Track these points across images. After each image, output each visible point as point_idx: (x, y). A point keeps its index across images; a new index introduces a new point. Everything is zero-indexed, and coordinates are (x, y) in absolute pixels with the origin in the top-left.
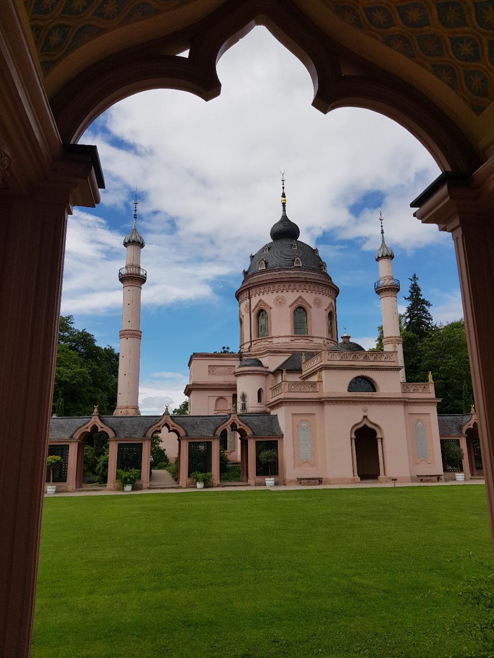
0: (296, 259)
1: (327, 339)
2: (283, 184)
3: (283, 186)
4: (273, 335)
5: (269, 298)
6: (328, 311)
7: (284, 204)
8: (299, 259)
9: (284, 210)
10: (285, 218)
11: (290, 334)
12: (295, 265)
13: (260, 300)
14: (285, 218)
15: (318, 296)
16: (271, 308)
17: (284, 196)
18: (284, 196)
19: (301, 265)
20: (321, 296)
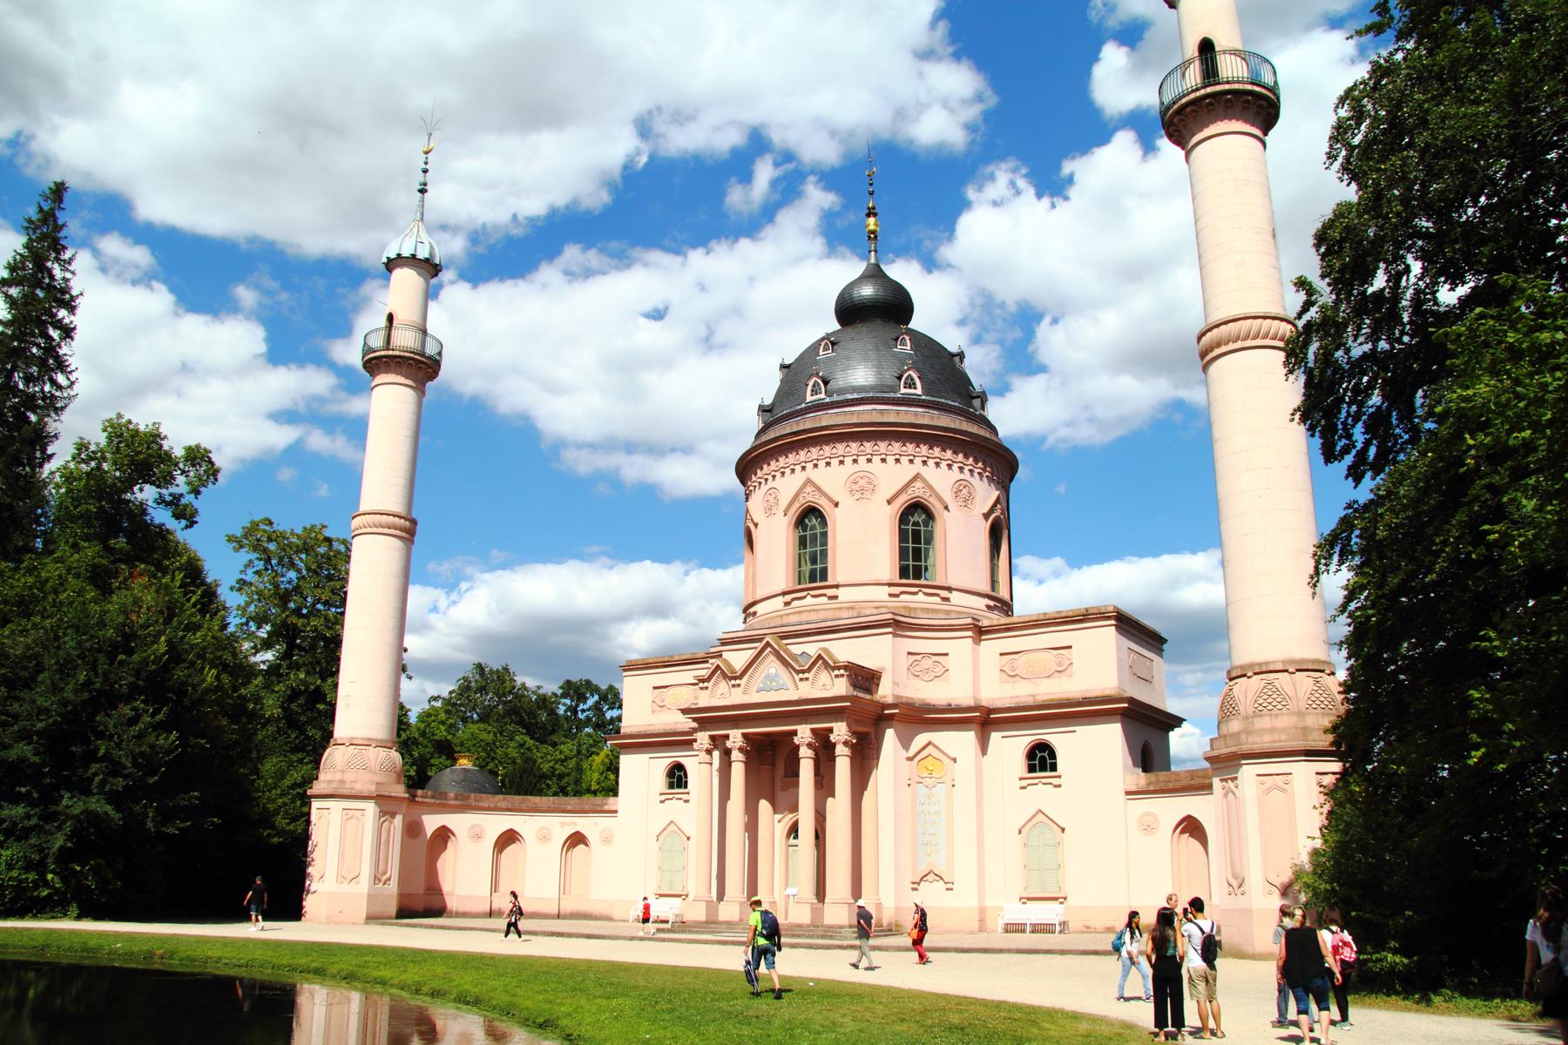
0: (811, 383)
11: (782, 585)
12: (809, 398)
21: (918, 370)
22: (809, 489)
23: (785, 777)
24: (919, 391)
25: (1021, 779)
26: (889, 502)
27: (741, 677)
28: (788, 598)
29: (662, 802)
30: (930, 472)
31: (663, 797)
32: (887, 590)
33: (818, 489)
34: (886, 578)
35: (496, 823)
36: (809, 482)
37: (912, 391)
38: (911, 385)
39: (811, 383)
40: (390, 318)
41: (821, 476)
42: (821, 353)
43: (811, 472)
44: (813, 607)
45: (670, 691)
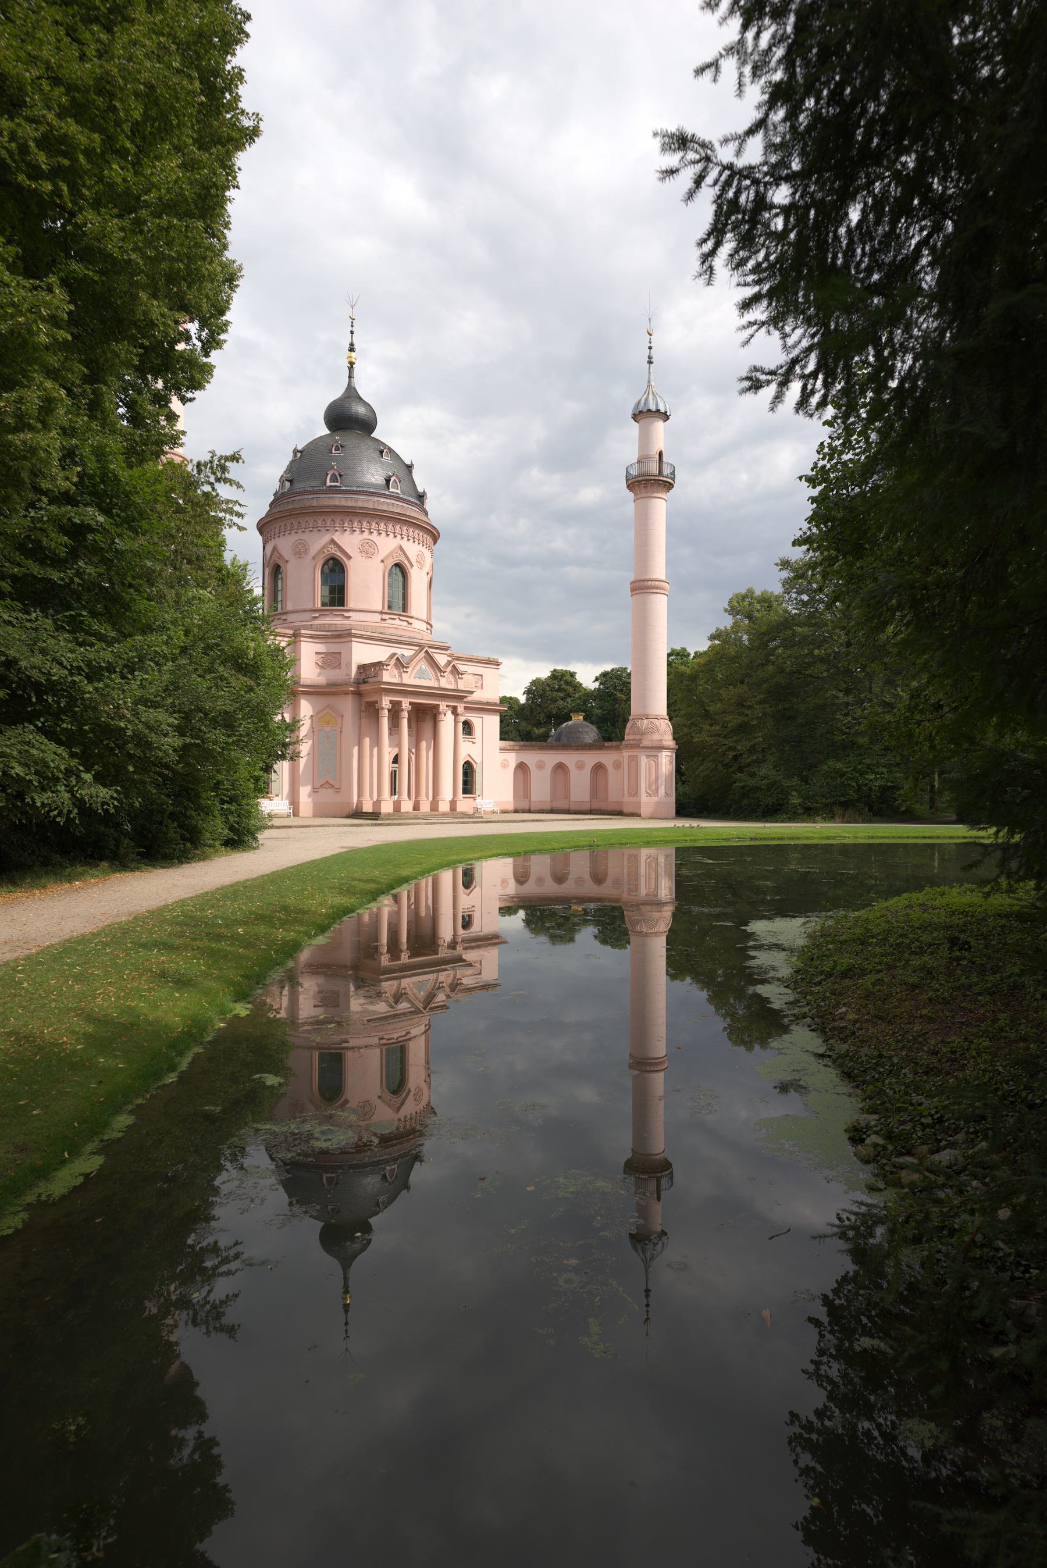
0: (330, 473)
1: (382, 613)
2: (352, 326)
3: (351, 328)
4: (290, 607)
5: (285, 544)
6: (391, 562)
8: (337, 474)
10: (351, 392)
11: (310, 606)
12: (329, 483)
13: (275, 549)
14: (351, 392)
15: (366, 535)
16: (287, 561)
17: (352, 349)
18: (352, 349)
20: (374, 537)
26: (382, 561)
30: (405, 544)
34: (379, 608)
36: (333, 541)
37: (396, 491)
41: (337, 537)
42: (333, 452)
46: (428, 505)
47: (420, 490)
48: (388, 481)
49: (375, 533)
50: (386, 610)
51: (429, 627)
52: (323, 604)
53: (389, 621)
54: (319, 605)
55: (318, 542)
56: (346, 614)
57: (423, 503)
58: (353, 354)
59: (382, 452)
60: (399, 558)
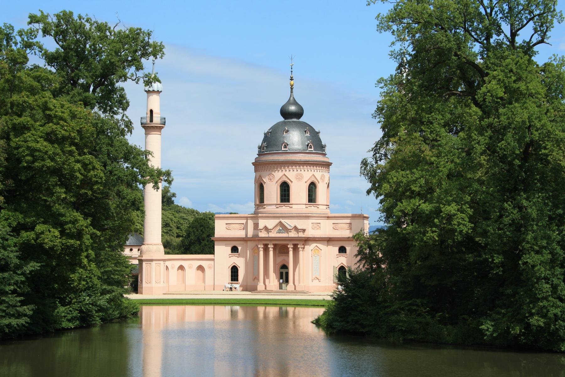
0: (283, 145)
1: (306, 204)
7: (292, 89)
9: (292, 92)
11: (276, 203)
12: (283, 149)
17: (292, 79)
19: (287, 149)
20: (302, 172)
21: (312, 144)
22: (284, 177)
23: (279, 253)
24: (312, 149)
25: (337, 255)
26: (306, 182)
27: (272, 229)
28: (278, 206)
29: (230, 257)
31: (230, 256)
32: (304, 206)
33: (287, 177)
34: (305, 203)
35: (179, 263)
38: (311, 148)
39: (283, 145)
40: (151, 111)
43: (284, 172)
44: (284, 209)
45: (232, 225)
46: (327, 150)
47: (323, 144)
48: (308, 145)
49: (303, 170)
50: (307, 203)
51: (327, 207)
52: (282, 200)
53: (309, 208)
54: (279, 202)
55: (279, 175)
56: (291, 206)
57: (324, 151)
58: (292, 82)
59: (306, 132)
60: (313, 179)
